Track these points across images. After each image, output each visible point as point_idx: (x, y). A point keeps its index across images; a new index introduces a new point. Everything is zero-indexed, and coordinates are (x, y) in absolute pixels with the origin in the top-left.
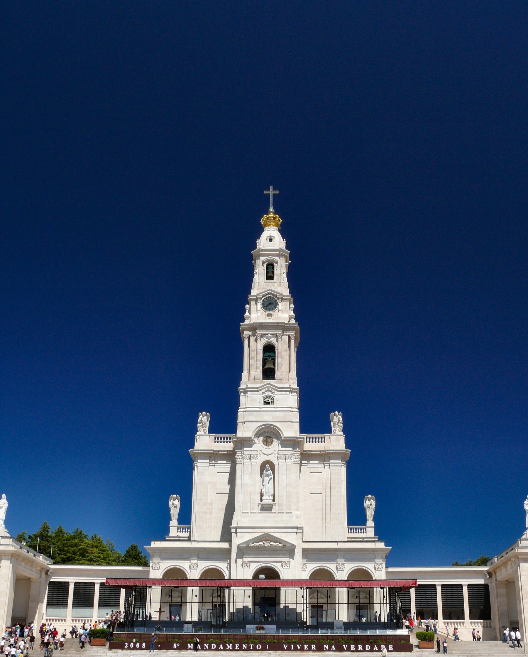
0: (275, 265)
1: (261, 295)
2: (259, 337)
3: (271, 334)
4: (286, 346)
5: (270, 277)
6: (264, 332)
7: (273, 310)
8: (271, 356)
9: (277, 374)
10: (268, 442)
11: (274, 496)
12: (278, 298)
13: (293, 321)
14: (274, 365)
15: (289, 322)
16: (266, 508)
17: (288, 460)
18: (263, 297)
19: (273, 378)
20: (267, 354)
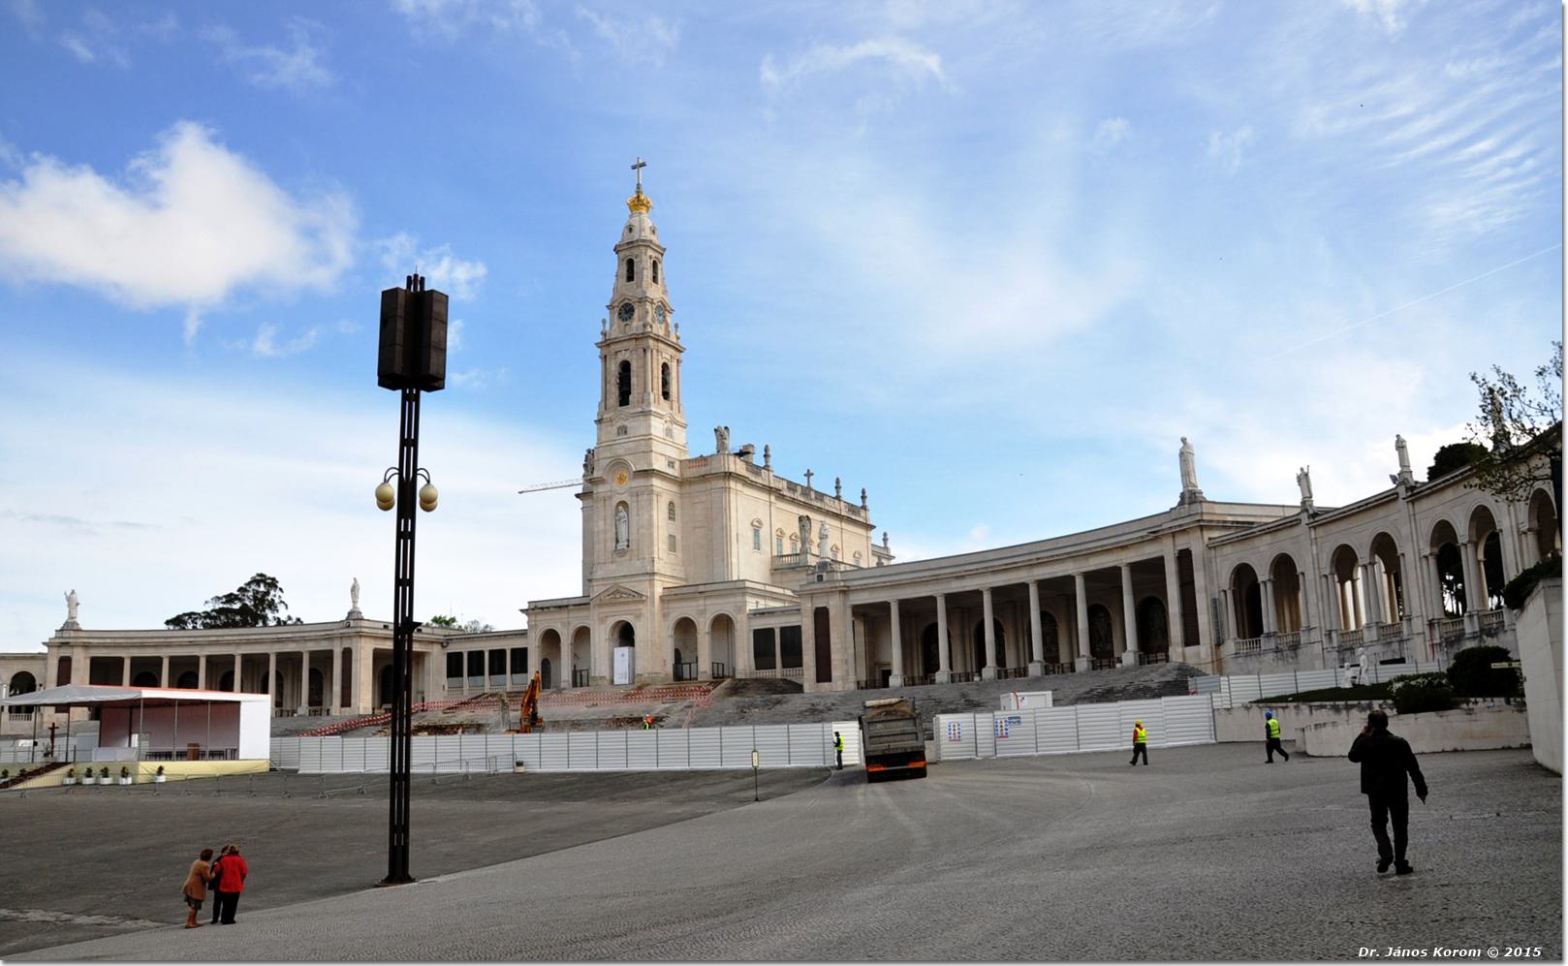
0: (635, 260)
1: (616, 304)
4: (641, 362)
6: (617, 347)
10: (621, 479)
11: (628, 541)
16: (620, 553)
17: (640, 498)
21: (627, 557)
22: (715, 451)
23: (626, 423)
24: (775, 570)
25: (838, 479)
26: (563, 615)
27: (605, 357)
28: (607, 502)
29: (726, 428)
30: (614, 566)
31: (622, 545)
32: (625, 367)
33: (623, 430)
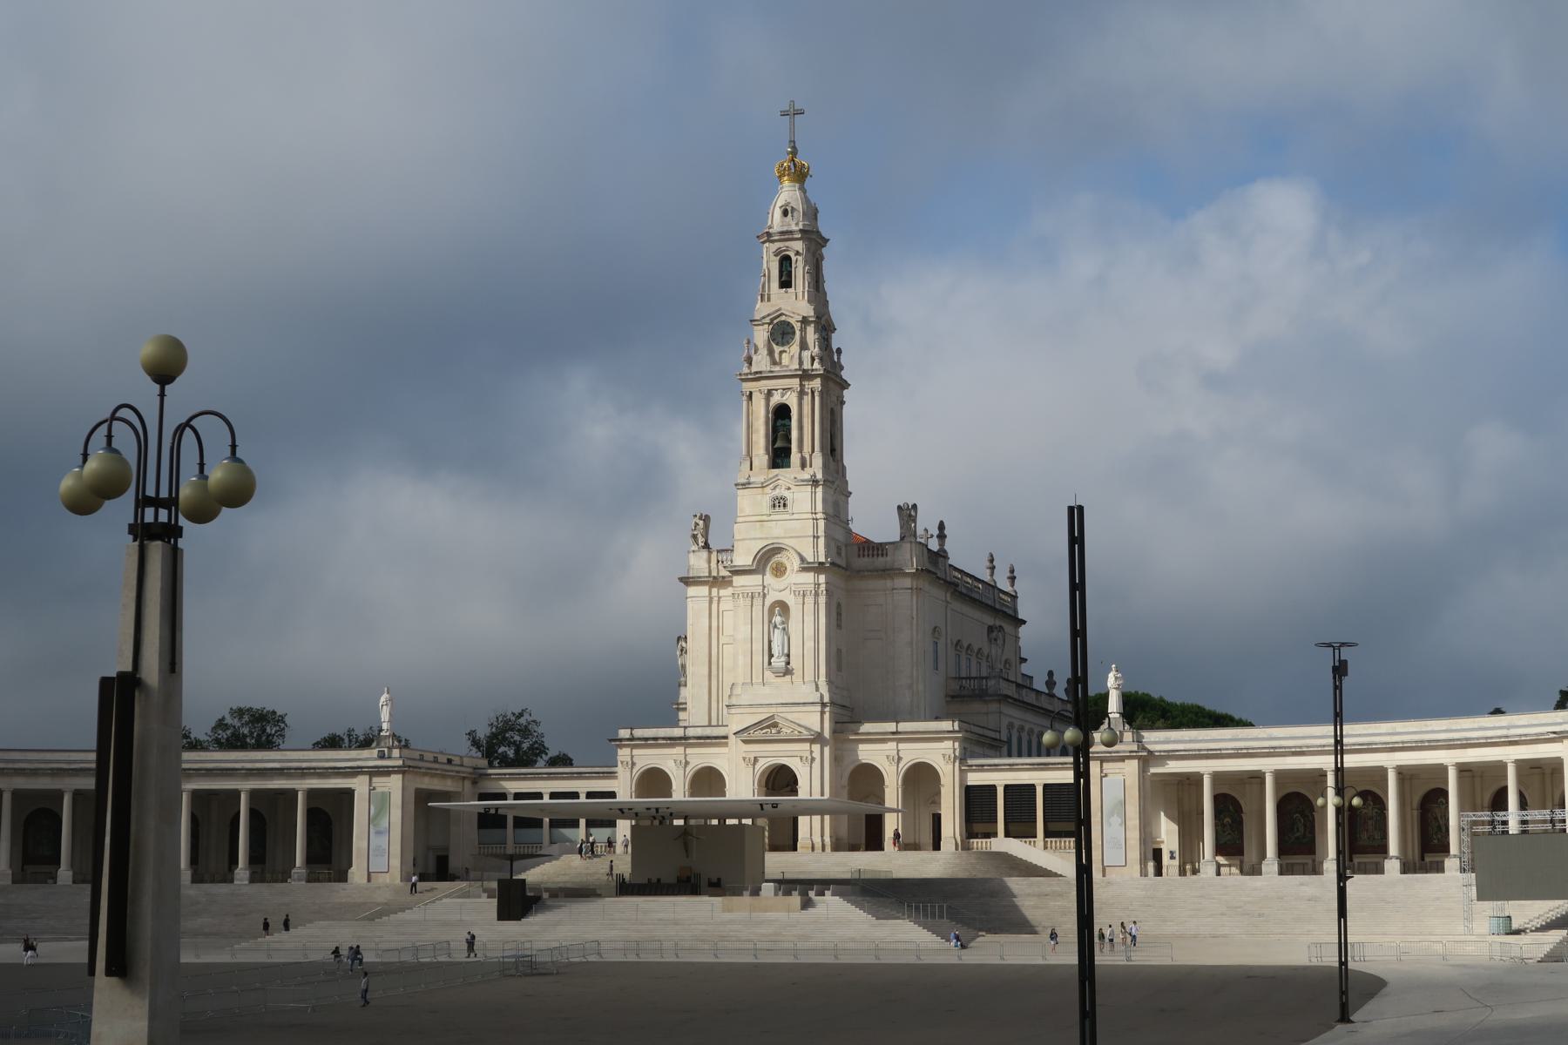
0: (794, 258)
1: (767, 320)
2: (763, 396)
3: (784, 389)
5: (786, 283)
7: (788, 343)
8: (784, 425)
9: (795, 457)
10: (780, 571)
11: (788, 656)
12: (798, 321)
13: (816, 365)
14: (791, 444)
15: (812, 365)
18: (772, 320)
19: (789, 467)
20: (779, 422)
21: (788, 677)
22: (898, 539)
23: (786, 494)
24: (953, 697)
25: (992, 556)
26: (678, 751)
27: (751, 393)
28: (758, 602)
29: (915, 506)
30: (767, 690)
31: (778, 662)
32: (782, 412)
33: (780, 503)
